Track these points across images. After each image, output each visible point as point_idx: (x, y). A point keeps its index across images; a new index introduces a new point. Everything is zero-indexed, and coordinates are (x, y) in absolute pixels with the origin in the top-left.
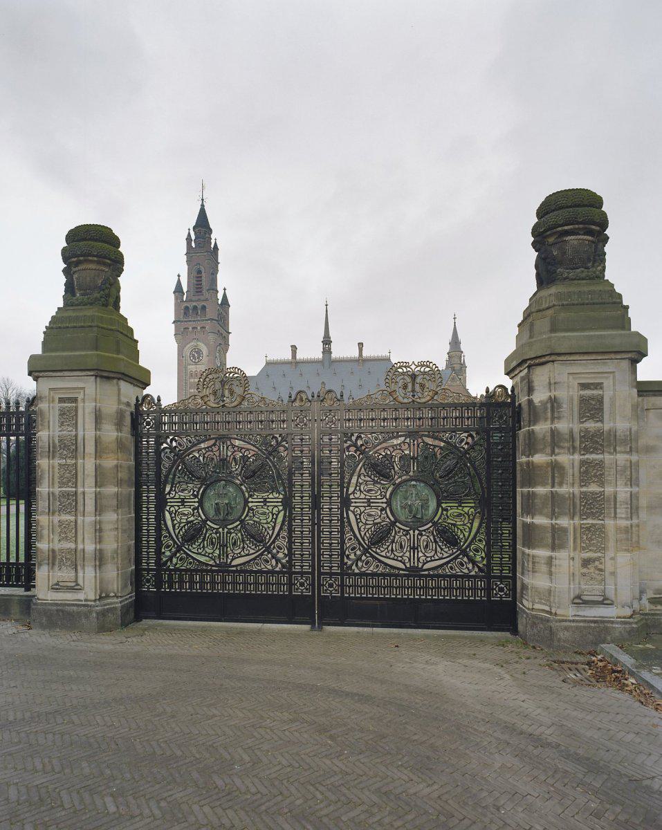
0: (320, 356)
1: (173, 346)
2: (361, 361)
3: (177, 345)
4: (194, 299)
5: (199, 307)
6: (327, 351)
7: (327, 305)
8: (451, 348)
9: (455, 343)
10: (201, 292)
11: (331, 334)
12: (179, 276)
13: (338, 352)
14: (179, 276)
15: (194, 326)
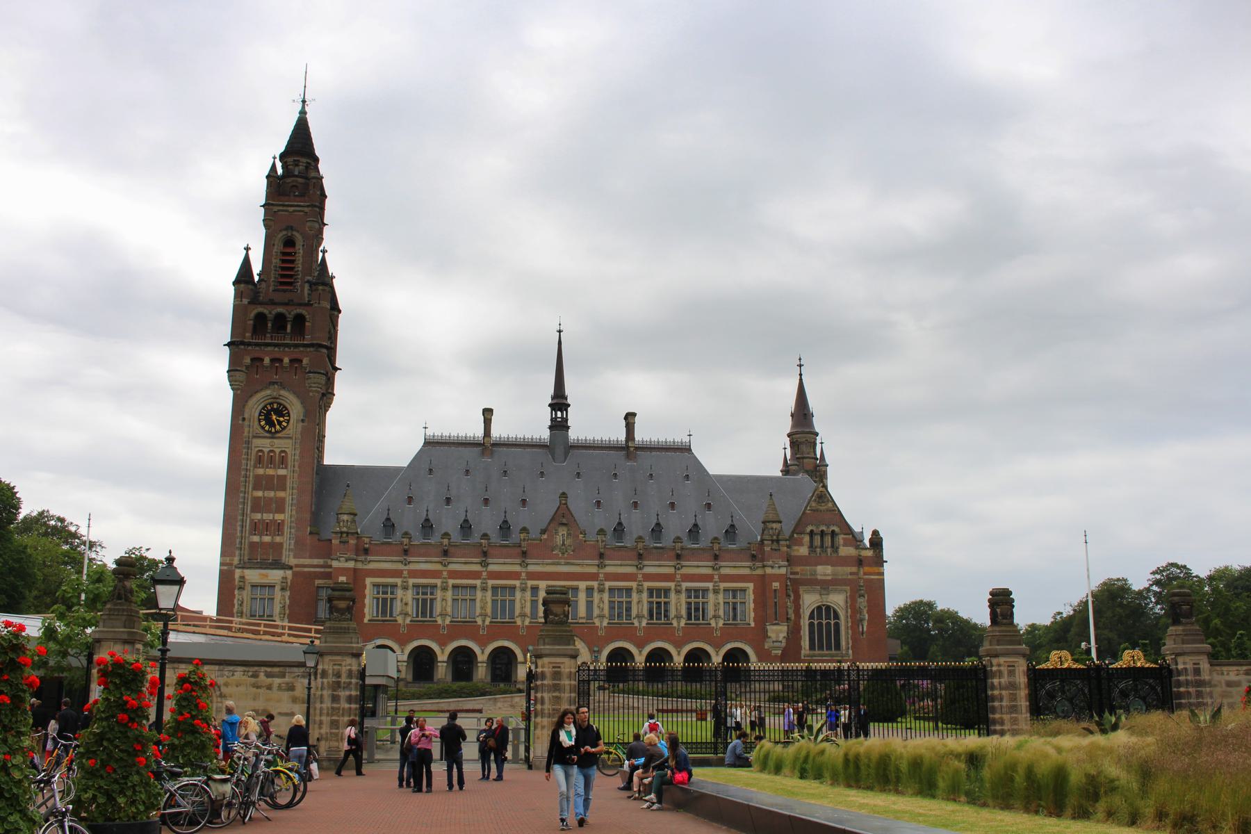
0: (541, 431)
1: (225, 397)
2: (629, 449)
3: (231, 393)
4: (278, 297)
5: (290, 317)
6: (559, 426)
7: (560, 331)
8: (793, 426)
9: (802, 413)
10: (290, 284)
11: (569, 390)
12: (247, 249)
13: (579, 430)
14: (247, 249)
15: (277, 356)
